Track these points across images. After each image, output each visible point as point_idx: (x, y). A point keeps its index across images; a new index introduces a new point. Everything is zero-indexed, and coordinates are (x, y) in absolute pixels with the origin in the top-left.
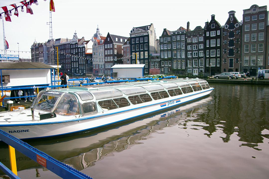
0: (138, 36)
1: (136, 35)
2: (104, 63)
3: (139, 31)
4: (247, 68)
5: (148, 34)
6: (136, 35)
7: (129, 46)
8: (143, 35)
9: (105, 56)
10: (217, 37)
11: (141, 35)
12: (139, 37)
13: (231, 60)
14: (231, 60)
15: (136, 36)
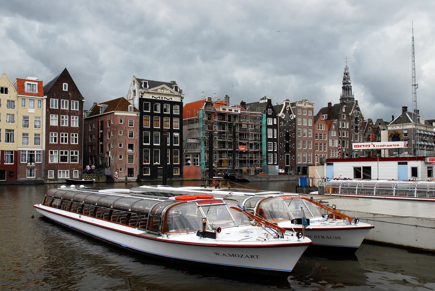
0: (158, 99)
1: (156, 96)
2: (44, 149)
3: (162, 91)
4: (301, 166)
5: (181, 100)
6: (156, 96)
7: (135, 115)
8: (170, 100)
9: (49, 129)
10: (273, 127)
11: (166, 100)
12: (162, 102)
13: (288, 156)
14: (288, 156)
15: (154, 98)
